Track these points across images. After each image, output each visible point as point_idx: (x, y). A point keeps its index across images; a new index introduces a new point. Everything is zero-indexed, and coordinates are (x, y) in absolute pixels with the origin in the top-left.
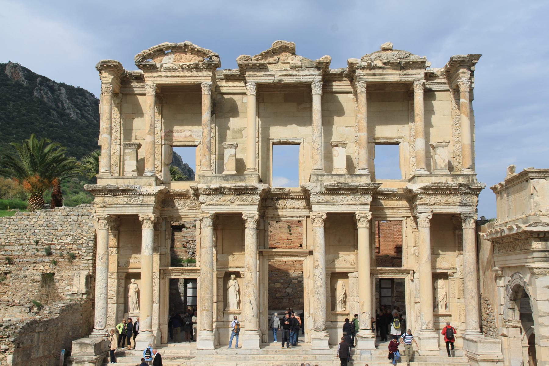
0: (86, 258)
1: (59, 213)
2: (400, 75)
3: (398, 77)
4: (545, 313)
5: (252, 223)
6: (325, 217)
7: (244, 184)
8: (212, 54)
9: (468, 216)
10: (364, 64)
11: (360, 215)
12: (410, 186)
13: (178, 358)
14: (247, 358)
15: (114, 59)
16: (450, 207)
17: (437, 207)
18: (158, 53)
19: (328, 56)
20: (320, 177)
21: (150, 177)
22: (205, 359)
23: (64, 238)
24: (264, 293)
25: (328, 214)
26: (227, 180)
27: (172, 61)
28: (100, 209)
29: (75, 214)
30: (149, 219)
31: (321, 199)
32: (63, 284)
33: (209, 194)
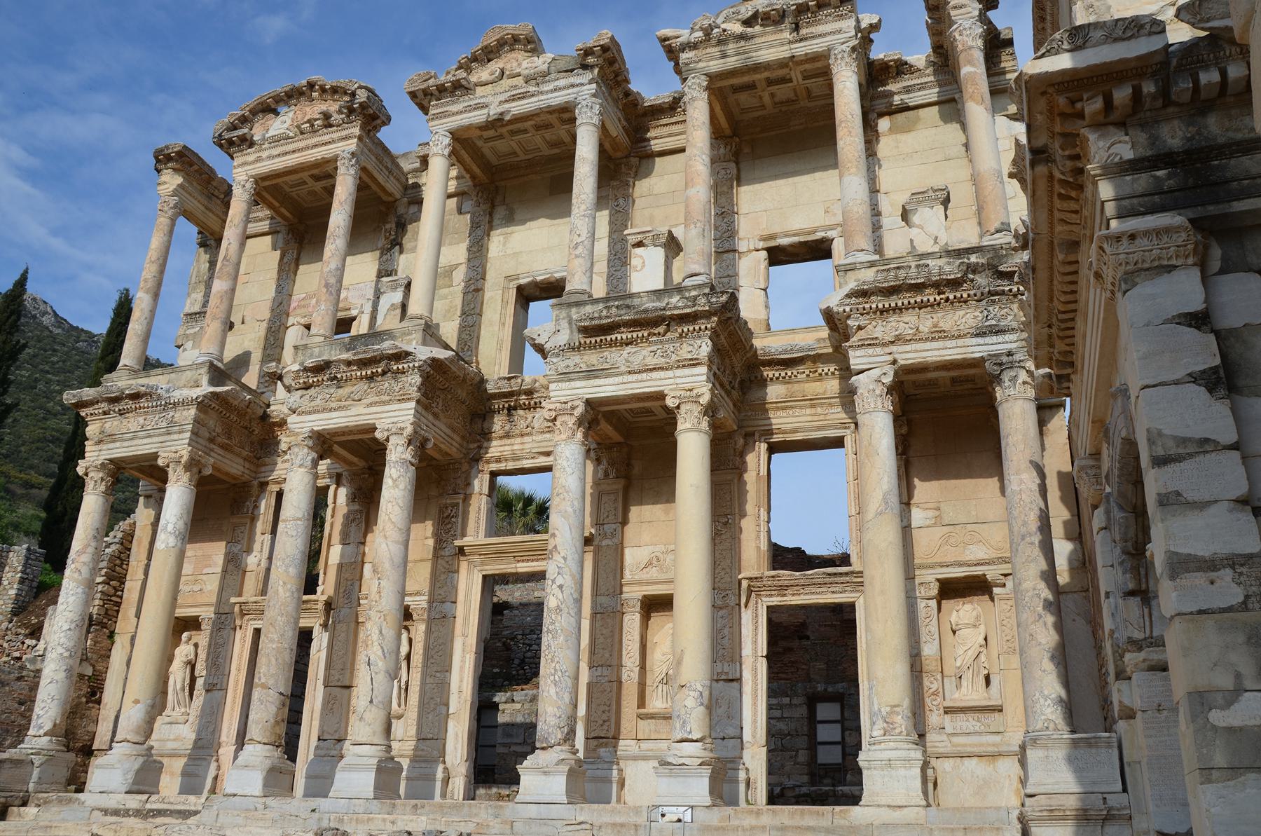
2: (790, 42)
3: (786, 47)
4: (1184, 441)
5: (400, 449)
6: (579, 411)
9: (1004, 363)
11: (677, 393)
15: (175, 142)
16: (948, 343)
17: (908, 348)
19: (605, 31)
20: (574, 310)
24: (463, 661)
25: (589, 403)
27: (286, 126)
28: (94, 448)
31: (571, 363)
33: (307, 387)
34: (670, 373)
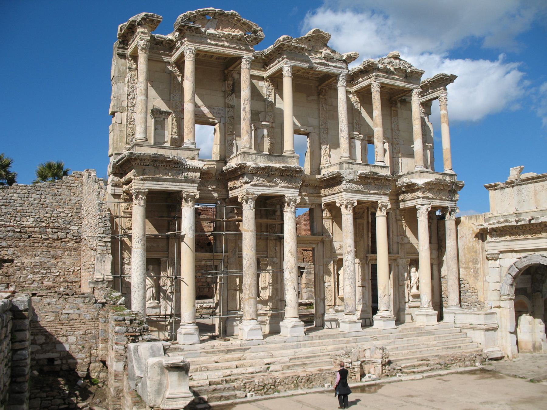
0: (104, 240)
1: (19, 191)
5: (294, 207)
6: (356, 204)
7: (293, 166)
8: (259, 28)
10: (380, 66)
12: (414, 181)
13: (234, 350)
14: (299, 346)
18: (202, 17)
20: (350, 165)
21: (193, 150)
22: (260, 350)
23: (25, 219)
26: (272, 161)
29: (38, 193)
30: (193, 197)
32: (25, 272)
33: (255, 174)
34: (380, 196)
